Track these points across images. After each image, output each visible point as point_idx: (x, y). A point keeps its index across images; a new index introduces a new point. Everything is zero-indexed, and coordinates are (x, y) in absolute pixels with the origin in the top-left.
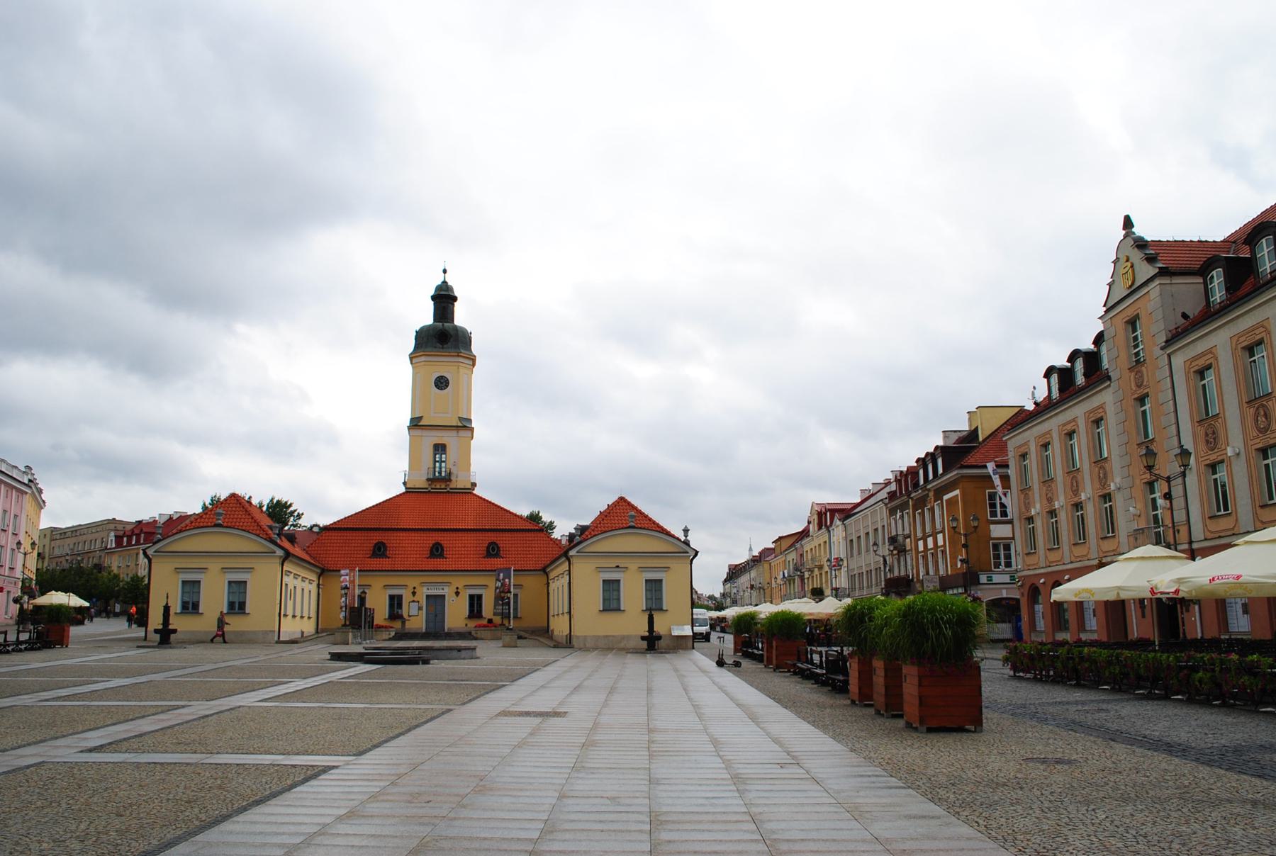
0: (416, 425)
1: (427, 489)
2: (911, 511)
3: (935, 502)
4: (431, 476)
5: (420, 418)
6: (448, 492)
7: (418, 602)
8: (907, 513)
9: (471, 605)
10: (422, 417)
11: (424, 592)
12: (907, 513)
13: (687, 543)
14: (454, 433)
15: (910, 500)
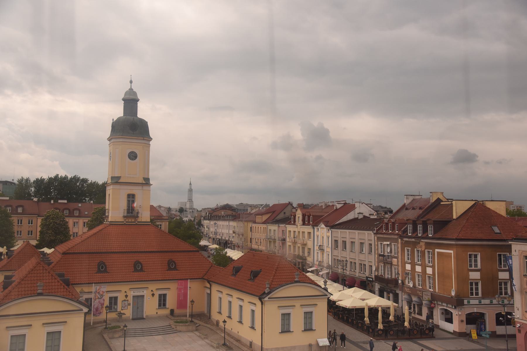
0: (117, 182)
1: (123, 222)
2: (400, 245)
3: (426, 249)
4: (126, 215)
5: (119, 178)
6: (137, 224)
7: (128, 300)
8: (395, 245)
9: (160, 300)
10: (121, 177)
11: (131, 294)
12: (395, 245)
13: (326, 289)
14: (140, 188)
15: (400, 240)
